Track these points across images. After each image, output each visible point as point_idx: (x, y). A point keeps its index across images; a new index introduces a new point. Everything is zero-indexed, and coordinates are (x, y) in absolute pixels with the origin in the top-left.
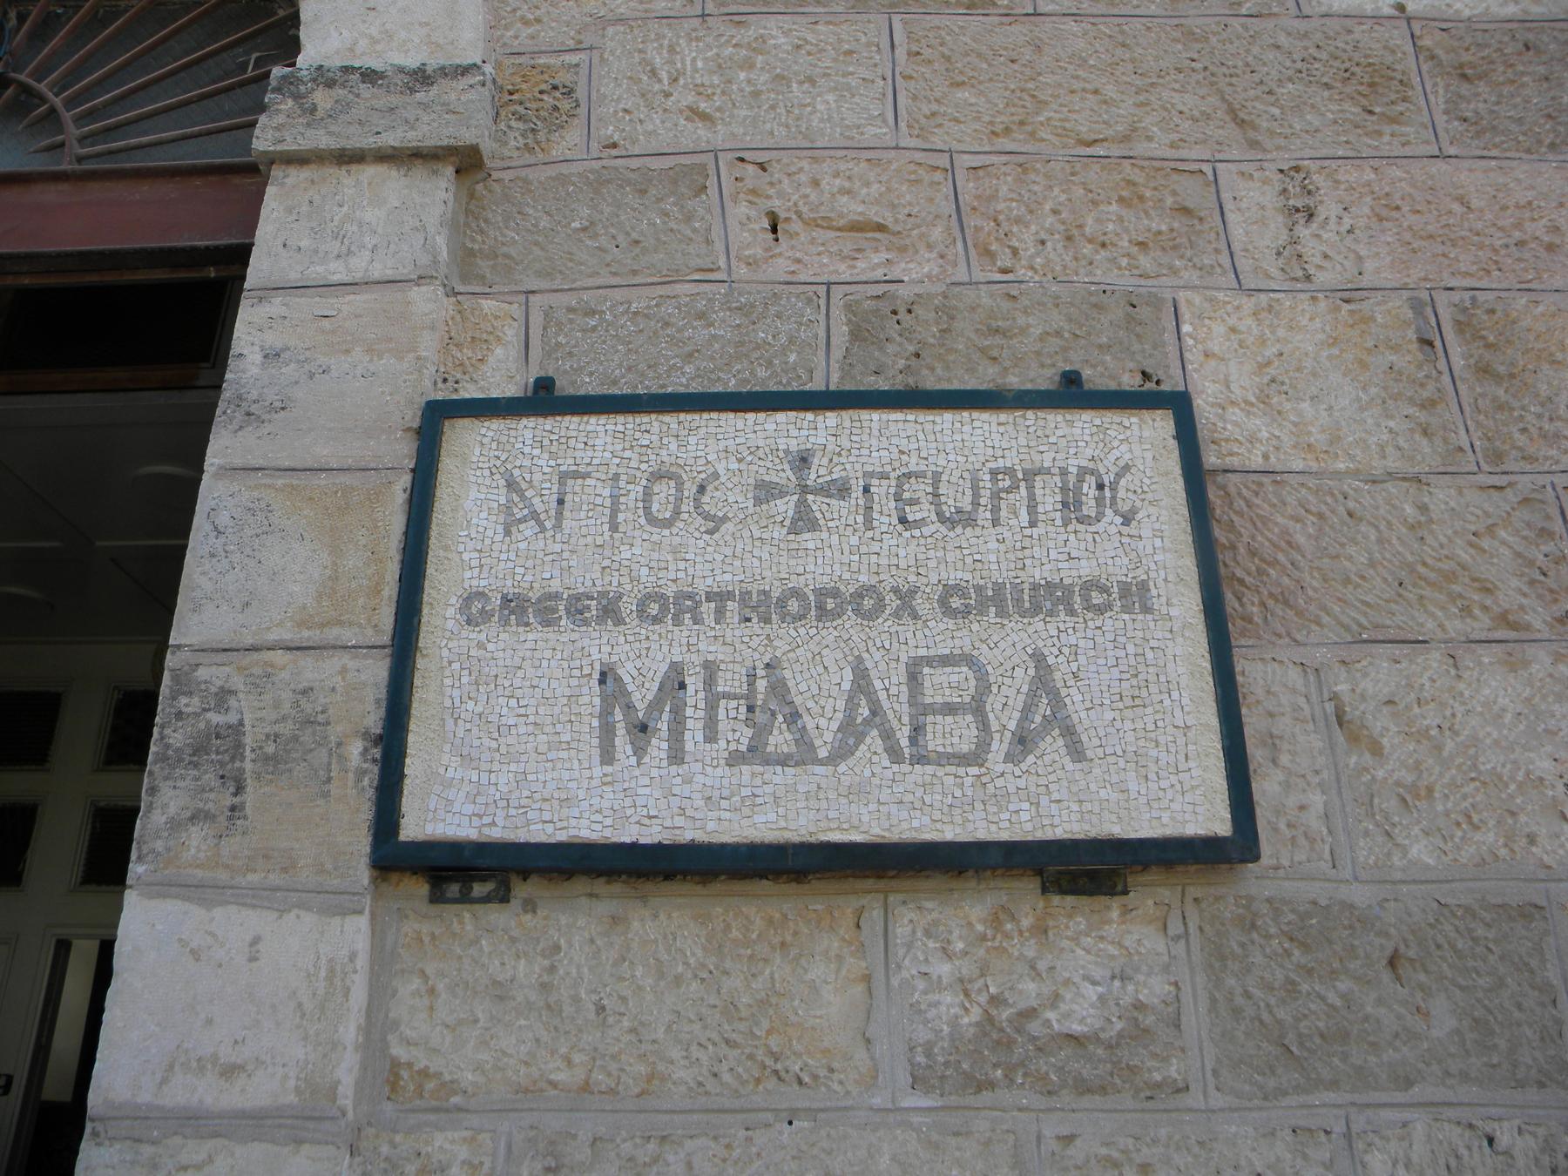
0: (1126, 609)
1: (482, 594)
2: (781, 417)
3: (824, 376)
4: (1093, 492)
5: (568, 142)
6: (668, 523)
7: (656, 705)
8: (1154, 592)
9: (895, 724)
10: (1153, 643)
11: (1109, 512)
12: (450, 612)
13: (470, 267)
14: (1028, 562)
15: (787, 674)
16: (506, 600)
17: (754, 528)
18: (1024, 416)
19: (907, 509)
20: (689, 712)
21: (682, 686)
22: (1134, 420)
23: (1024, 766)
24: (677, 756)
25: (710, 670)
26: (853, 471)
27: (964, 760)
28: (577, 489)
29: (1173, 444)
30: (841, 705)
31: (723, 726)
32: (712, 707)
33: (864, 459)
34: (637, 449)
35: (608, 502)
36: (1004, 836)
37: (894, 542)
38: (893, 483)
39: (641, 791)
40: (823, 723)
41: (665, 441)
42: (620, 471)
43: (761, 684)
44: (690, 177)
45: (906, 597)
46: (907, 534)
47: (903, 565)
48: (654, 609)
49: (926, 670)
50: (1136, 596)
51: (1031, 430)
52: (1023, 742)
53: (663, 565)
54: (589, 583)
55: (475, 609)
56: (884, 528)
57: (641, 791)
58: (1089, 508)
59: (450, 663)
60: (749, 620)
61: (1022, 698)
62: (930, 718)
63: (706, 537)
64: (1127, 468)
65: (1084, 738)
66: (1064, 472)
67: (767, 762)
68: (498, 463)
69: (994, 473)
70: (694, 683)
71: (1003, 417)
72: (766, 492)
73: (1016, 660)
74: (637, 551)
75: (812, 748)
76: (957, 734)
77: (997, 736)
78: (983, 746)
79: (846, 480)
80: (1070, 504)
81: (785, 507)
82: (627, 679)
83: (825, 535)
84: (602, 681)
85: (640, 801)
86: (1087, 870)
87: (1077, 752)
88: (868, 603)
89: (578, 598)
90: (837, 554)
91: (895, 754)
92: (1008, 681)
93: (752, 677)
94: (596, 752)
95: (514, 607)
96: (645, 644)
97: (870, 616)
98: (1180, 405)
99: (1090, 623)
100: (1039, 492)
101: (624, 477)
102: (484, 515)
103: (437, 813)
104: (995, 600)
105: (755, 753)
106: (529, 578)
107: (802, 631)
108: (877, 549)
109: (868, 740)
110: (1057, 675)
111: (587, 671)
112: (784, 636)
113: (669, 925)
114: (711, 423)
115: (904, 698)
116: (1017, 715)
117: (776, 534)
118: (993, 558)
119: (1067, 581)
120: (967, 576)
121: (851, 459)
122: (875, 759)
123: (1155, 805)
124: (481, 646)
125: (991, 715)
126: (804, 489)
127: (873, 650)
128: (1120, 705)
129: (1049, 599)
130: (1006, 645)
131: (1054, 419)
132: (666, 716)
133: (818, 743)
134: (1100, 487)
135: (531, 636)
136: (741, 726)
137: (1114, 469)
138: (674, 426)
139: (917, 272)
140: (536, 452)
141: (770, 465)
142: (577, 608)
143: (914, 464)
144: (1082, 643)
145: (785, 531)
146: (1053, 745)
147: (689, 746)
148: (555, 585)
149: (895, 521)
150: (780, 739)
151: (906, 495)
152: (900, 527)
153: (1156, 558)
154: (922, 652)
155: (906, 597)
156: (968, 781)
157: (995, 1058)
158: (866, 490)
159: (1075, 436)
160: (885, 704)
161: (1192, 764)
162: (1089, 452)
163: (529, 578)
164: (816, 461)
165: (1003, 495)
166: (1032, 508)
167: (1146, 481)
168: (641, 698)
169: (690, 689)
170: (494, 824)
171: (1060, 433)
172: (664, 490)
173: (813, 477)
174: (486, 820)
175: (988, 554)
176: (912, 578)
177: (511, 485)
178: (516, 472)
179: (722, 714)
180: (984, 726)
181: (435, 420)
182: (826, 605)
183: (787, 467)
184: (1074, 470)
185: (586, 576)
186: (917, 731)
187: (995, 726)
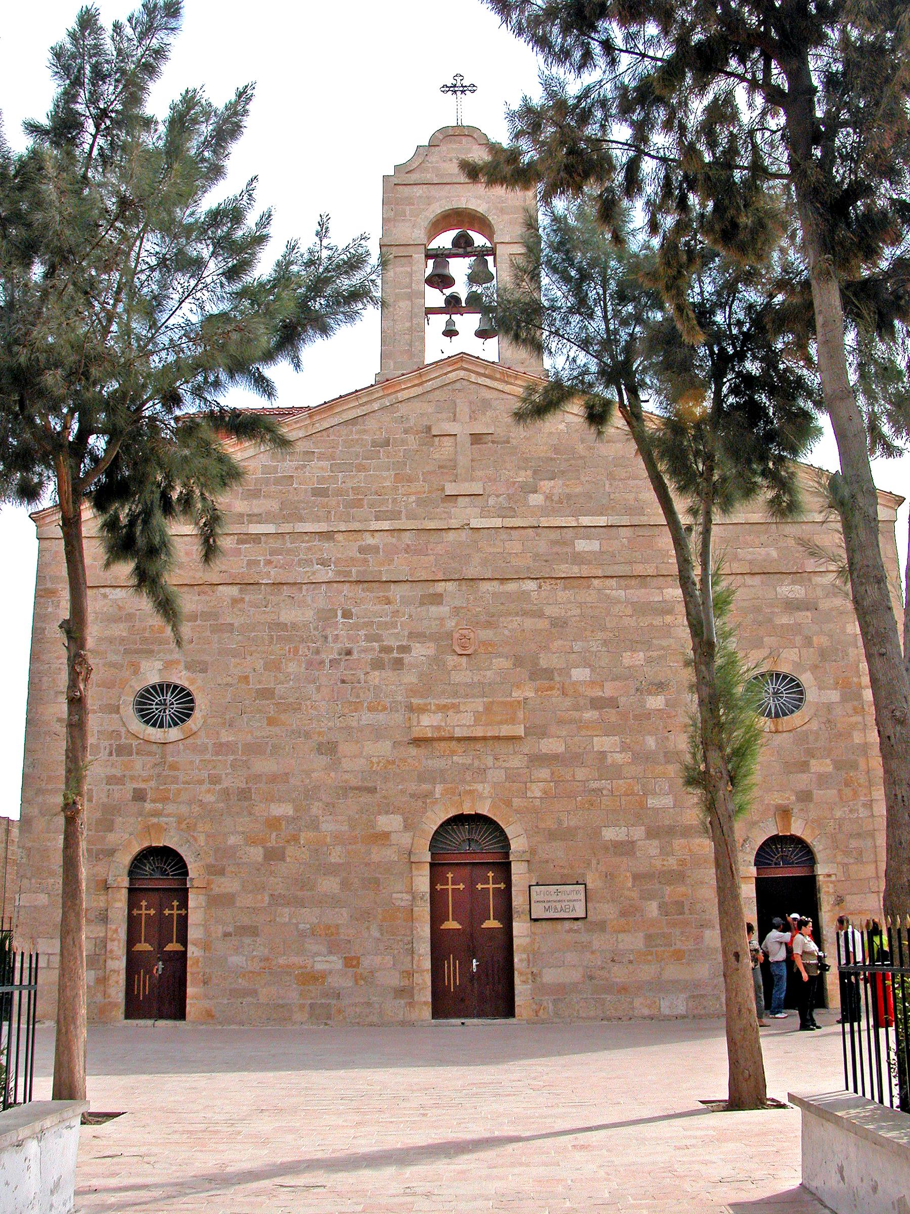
5: (537, 857)
13: (530, 871)
44: (547, 862)
86: (577, 919)
98: (585, 884)
104: (570, 901)
113: (549, 922)
130: (571, 904)
139: (566, 871)
157: (569, 931)
175: (570, 897)
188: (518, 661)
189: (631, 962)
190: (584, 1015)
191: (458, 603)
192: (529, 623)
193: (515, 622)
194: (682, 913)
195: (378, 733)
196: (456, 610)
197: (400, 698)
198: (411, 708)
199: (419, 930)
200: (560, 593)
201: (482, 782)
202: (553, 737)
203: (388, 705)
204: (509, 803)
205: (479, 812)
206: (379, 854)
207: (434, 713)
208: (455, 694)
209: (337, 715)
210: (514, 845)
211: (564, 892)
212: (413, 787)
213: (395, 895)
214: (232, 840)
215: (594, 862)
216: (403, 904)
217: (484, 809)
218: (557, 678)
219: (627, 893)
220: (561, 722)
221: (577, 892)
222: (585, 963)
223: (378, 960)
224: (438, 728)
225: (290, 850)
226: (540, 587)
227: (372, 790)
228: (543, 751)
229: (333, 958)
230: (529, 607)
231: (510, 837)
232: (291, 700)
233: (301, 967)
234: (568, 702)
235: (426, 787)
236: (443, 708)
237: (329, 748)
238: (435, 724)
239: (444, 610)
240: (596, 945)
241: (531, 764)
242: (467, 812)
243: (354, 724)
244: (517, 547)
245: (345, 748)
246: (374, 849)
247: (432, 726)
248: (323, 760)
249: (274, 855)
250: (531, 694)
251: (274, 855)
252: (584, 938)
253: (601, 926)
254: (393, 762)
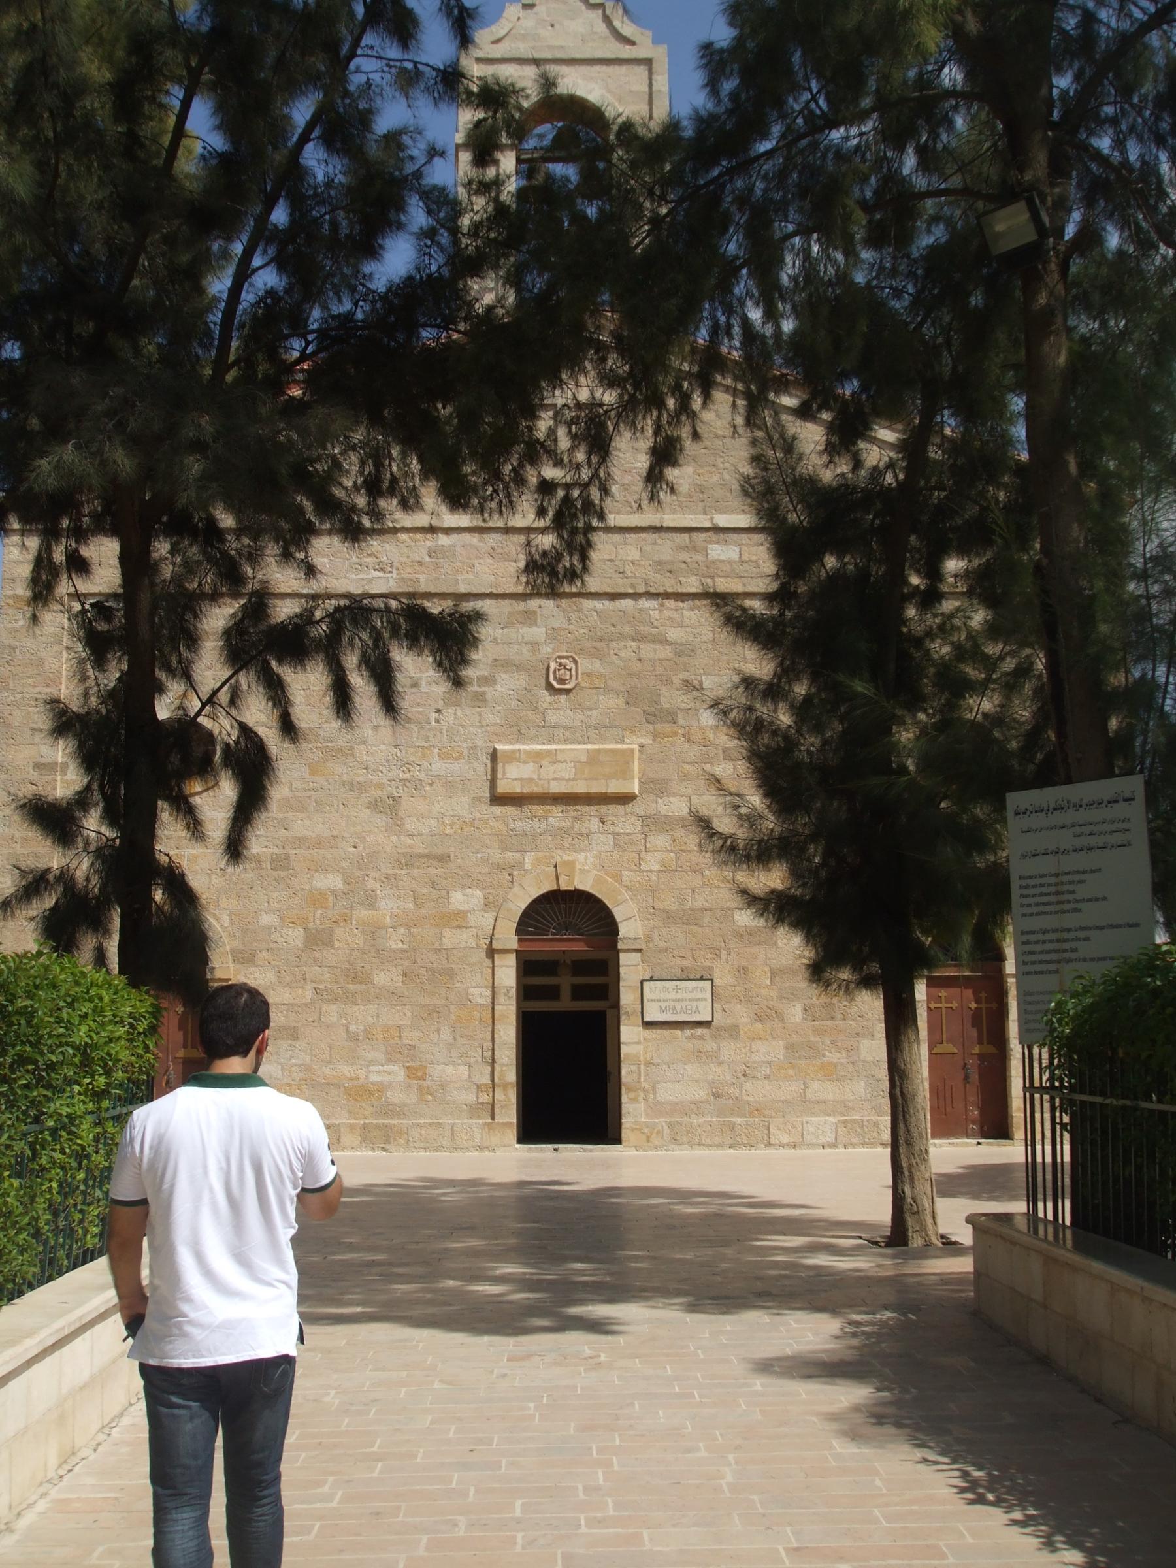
3: (679, 975)
44: (666, 950)
86: (700, 1024)
98: (712, 980)
103: (647, 1018)
130: (694, 1004)
139: (687, 963)
159: (701, 983)
175: (692, 996)
181: (642, 982)
188: (631, 698)
189: (767, 1077)
190: (708, 1141)
191: (557, 625)
192: (646, 650)
193: (627, 651)
194: (832, 1018)
195: (450, 786)
196: (553, 634)
197: (479, 743)
198: (494, 756)
199: (502, 1033)
200: (687, 613)
201: (584, 851)
202: (675, 795)
203: (466, 751)
204: (619, 878)
205: (581, 887)
206: (450, 938)
207: (525, 762)
208: (552, 740)
209: (399, 763)
210: (624, 930)
212: (496, 855)
213: (472, 990)
214: (265, 919)
215: (724, 952)
216: (482, 1001)
217: (586, 885)
218: (681, 722)
219: (764, 991)
220: (685, 778)
221: (702, 990)
222: (710, 1078)
223: (450, 1070)
224: (531, 780)
225: (339, 932)
226: (662, 605)
227: (444, 859)
228: (664, 812)
229: (390, 1067)
230: (644, 629)
231: (618, 920)
232: (341, 743)
233: (351, 1079)
234: (693, 752)
235: (510, 855)
236: (537, 757)
237: (389, 806)
238: (525, 777)
239: (537, 632)
240: (725, 1056)
241: (646, 829)
242: (563, 887)
243: (422, 776)
244: (634, 554)
245: (409, 803)
246: (447, 933)
247: (521, 779)
248: (381, 821)
249: (317, 939)
250: (647, 741)
251: (317, 939)
252: (710, 1046)
253: (733, 1031)
254: (472, 823)
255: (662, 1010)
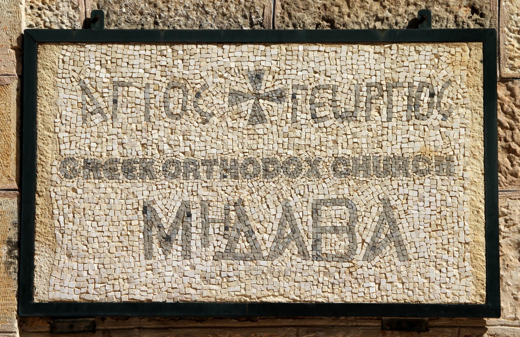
0: (438, 173)
1: (73, 159)
2: (244, 47)
4: (427, 99)
6: (178, 116)
7: (174, 227)
8: (456, 162)
9: (305, 239)
10: (452, 194)
11: (435, 112)
12: (54, 170)
14: (384, 143)
15: (247, 209)
16: (87, 163)
17: (229, 120)
18: (390, 48)
19: (317, 109)
20: (193, 230)
21: (189, 215)
22: (458, 49)
23: (374, 263)
24: (187, 254)
25: (205, 205)
26: (286, 84)
27: (342, 258)
28: (125, 93)
29: (480, 66)
30: (276, 227)
31: (213, 239)
32: (205, 227)
33: (293, 77)
34: (159, 68)
35: (143, 102)
36: (360, 301)
37: (308, 130)
38: (310, 92)
39: (167, 274)
40: (266, 236)
41: (176, 62)
42: (151, 82)
43: (233, 214)
45: (313, 164)
46: (316, 126)
47: (313, 145)
48: (173, 170)
49: (324, 208)
50: (445, 164)
51: (394, 57)
52: (374, 248)
53: (177, 143)
54: (134, 153)
55: (69, 168)
56: (303, 122)
57: (167, 274)
58: (424, 109)
59: (57, 201)
60: (225, 177)
61: (375, 224)
62: (324, 235)
63: (201, 126)
64: (449, 82)
65: (408, 247)
66: (410, 86)
67: (235, 258)
68: (75, 75)
69: (369, 86)
70: (195, 213)
71: (378, 48)
72: (236, 96)
73: (372, 202)
74: (162, 133)
75: (259, 251)
76: (339, 244)
77: (360, 245)
78: (352, 250)
79: (282, 91)
80: (413, 104)
81: (247, 106)
82: (158, 210)
83: (268, 125)
84: (145, 212)
85: (167, 279)
87: (403, 255)
88: (292, 168)
89: (130, 162)
90: (276, 136)
91: (304, 254)
92: (368, 214)
93: (227, 210)
94: (142, 252)
95: (92, 167)
96: (168, 191)
97: (293, 175)
98: (488, 40)
99: (417, 182)
100: (394, 98)
101: (152, 86)
102: (69, 109)
105: (230, 252)
106: (99, 149)
107: (255, 184)
108: (299, 135)
109: (290, 247)
110: (396, 212)
111: (136, 206)
112: (245, 190)
114: (203, 51)
115: (310, 223)
116: (371, 234)
117: (241, 125)
118: (364, 140)
119: (406, 156)
120: (349, 152)
121: (286, 76)
122: (294, 257)
123: (443, 286)
124: (74, 190)
125: (357, 234)
126: (258, 97)
127: (294, 195)
128: (430, 229)
129: (392, 166)
130: (369, 194)
131: (407, 48)
132: (180, 232)
133: (263, 247)
134: (432, 95)
135: (102, 185)
136: (220, 238)
137: (441, 83)
138: (181, 52)
140: (98, 68)
141: (238, 80)
142: (128, 169)
143: (322, 80)
144: (411, 193)
145: (246, 122)
146: (389, 251)
147: (193, 249)
148: (116, 154)
149: (309, 117)
150: (242, 246)
151: (317, 100)
152: (312, 121)
153: (460, 141)
154: (321, 197)
155: (313, 164)
156: (343, 270)
158: (294, 97)
160: (300, 226)
161: (466, 264)
162: (428, 72)
163: (99, 149)
164: (265, 77)
165: (373, 101)
166: (389, 110)
167: (461, 91)
168: (167, 222)
169: (194, 217)
170: (88, 293)
171: (411, 59)
172: (177, 95)
173: (263, 88)
174: (83, 290)
175: (361, 138)
176: (318, 153)
177: (84, 89)
178: (87, 81)
179: (211, 231)
180: (353, 240)
182: (269, 168)
183: (248, 81)
184: (416, 84)
185: (134, 151)
186: (317, 241)
187: (359, 239)
211: (317, 101)
255: (161, 234)
